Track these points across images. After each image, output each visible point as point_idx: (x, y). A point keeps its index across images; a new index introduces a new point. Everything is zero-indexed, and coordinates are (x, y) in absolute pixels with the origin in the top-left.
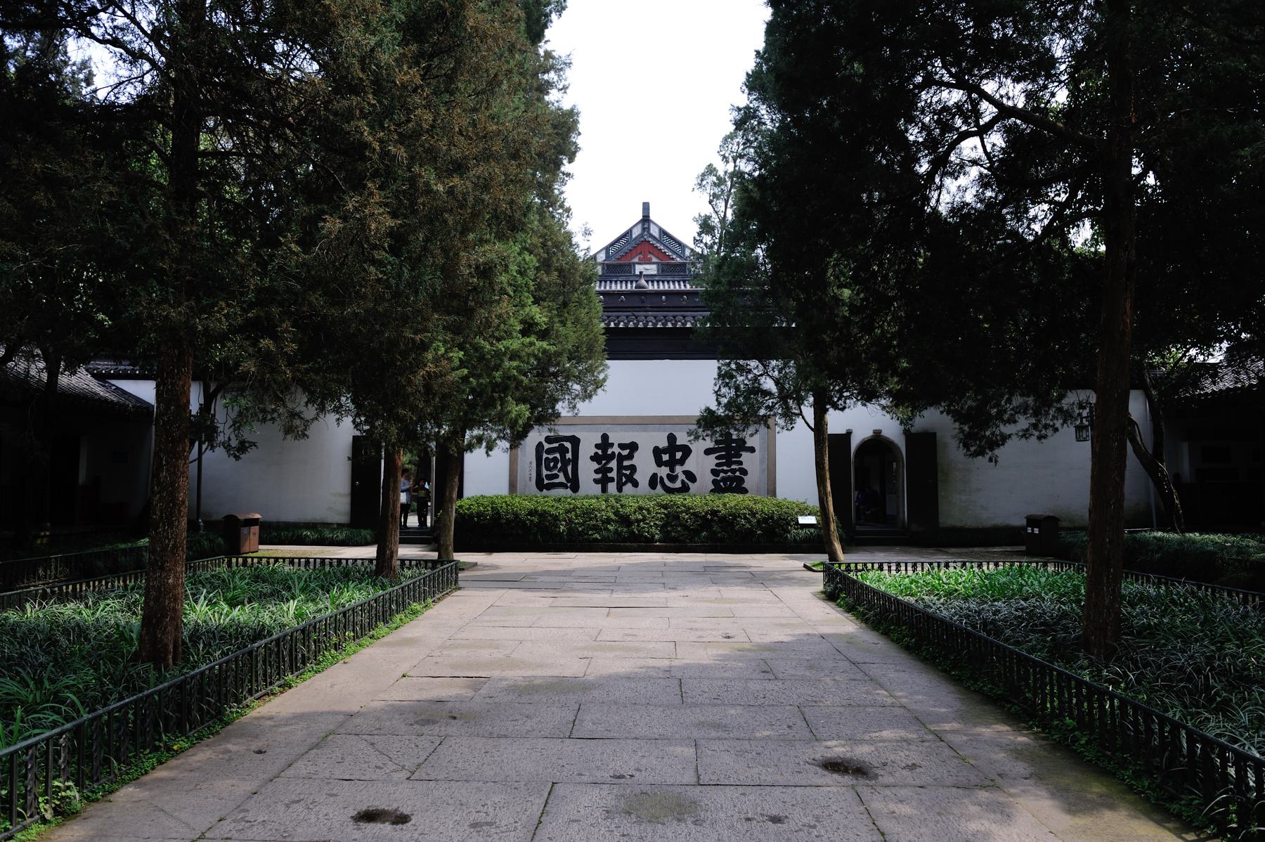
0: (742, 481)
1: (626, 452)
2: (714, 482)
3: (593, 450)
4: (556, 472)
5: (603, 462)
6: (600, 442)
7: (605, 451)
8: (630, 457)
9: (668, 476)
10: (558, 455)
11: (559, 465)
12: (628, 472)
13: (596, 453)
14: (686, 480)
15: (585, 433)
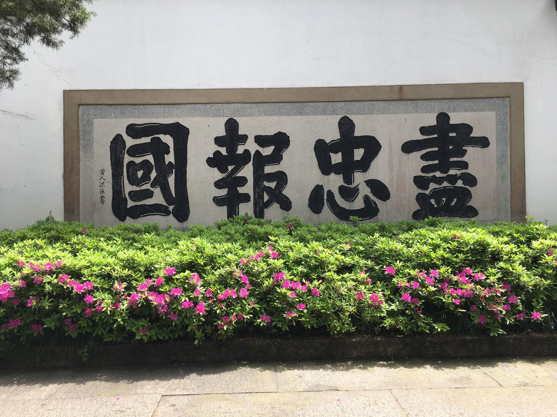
0: (466, 195)
1: (267, 151)
2: (420, 198)
3: (212, 149)
4: (147, 186)
5: (230, 168)
6: (222, 132)
7: (232, 149)
8: (276, 158)
9: (342, 190)
10: (150, 158)
11: (153, 175)
12: (273, 185)
13: (217, 153)
14: (372, 197)
15: (197, 119)
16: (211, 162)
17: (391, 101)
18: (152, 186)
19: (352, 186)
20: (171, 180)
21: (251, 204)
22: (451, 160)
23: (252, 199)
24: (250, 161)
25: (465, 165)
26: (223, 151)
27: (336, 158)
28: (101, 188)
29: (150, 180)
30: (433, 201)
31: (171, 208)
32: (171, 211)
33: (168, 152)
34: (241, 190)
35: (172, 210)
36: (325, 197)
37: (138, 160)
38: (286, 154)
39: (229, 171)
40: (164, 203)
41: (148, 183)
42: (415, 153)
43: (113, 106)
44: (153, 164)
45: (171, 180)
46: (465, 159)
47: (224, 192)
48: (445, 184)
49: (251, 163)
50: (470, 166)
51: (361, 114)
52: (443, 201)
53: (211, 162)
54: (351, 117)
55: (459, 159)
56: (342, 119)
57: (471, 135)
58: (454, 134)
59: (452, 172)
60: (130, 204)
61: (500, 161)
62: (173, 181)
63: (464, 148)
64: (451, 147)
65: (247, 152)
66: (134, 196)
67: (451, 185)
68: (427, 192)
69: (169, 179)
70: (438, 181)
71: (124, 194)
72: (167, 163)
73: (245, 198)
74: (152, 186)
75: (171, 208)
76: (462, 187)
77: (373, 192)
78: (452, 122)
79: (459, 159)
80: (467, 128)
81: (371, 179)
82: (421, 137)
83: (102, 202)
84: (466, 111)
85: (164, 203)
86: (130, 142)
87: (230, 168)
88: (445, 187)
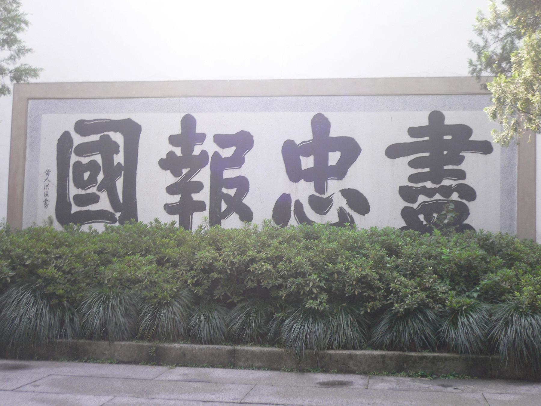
1: (228, 153)
2: (406, 213)
4: (93, 190)
5: (185, 171)
6: (177, 130)
7: (187, 149)
10: (98, 158)
11: (100, 177)
12: (232, 192)
16: (164, 164)
17: (374, 96)
18: (99, 189)
19: (324, 196)
20: (120, 183)
21: (206, 213)
22: (446, 167)
23: (208, 208)
24: (207, 164)
25: (462, 175)
26: (178, 151)
27: (307, 163)
28: (45, 190)
29: (97, 183)
30: (421, 217)
32: (118, 219)
33: (117, 152)
34: (196, 197)
35: (119, 217)
36: (293, 208)
37: (85, 160)
38: (249, 157)
39: (183, 175)
40: (111, 210)
41: (95, 186)
42: (402, 159)
43: (62, 101)
44: (101, 164)
45: (120, 183)
46: (462, 167)
47: (176, 199)
48: (438, 197)
49: (208, 166)
50: (468, 176)
51: (339, 111)
52: (434, 217)
53: (164, 164)
54: (327, 114)
55: (455, 167)
56: (315, 116)
57: (471, 139)
58: (449, 137)
59: (446, 182)
60: (75, 209)
61: (506, 171)
63: (461, 154)
64: (445, 153)
65: (204, 153)
66: (80, 200)
67: (444, 199)
68: (415, 206)
69: (117, 182)
70: (429, 193)
72: (115, 164)
73: (200, 207)
74: (99, 189)
75: (118, 215)
76: (458, 201)
77: (349, 203)
78: (447, 122)
79: (455, 167)
80: (466, 131)
81: (347, 188)
82: (409, 140)
83: (46, 206)
84: (465, 109)
85: (111, 210)
86: (78, 140)
87: (185, 171)
88: (437, 200)
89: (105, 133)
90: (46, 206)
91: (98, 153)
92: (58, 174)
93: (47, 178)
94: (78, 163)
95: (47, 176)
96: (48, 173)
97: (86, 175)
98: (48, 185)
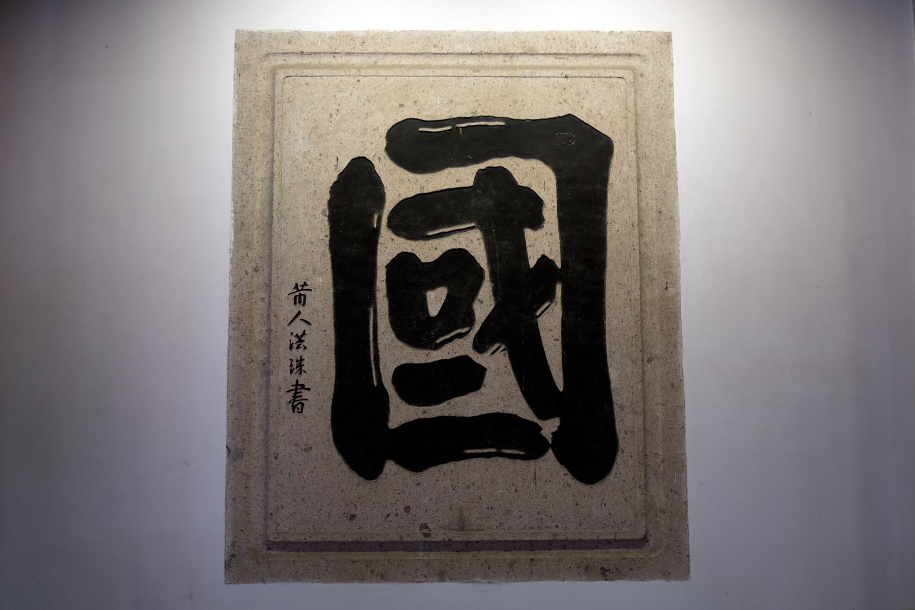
18: (480, 345)
31: (549, 427)
33: (537, 222)
40: (521, 408)
62: (558, 332)
71: (379, 375)
72: (532, 263)
74: (480, 345)
75: (549, 427)
83: (297, 404)
85: (521, 408)
89: (494, 162)
90: (297, 404)
91: (473, 224)
92: (337, 296)
93: (299, 313)
94: (404, 261)
95: (299, 307)
96: (300, 295)
97: (436, 300)
98: (304, 334)
